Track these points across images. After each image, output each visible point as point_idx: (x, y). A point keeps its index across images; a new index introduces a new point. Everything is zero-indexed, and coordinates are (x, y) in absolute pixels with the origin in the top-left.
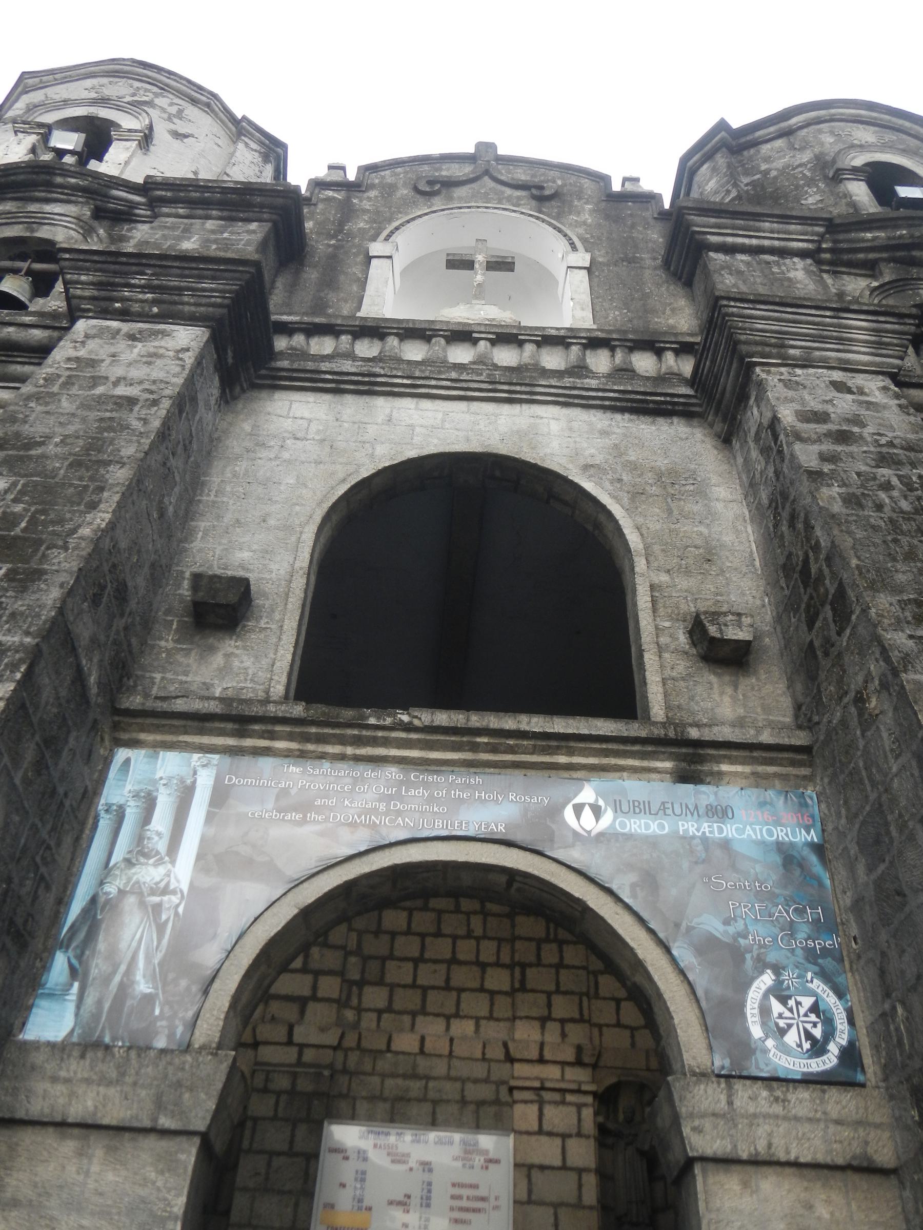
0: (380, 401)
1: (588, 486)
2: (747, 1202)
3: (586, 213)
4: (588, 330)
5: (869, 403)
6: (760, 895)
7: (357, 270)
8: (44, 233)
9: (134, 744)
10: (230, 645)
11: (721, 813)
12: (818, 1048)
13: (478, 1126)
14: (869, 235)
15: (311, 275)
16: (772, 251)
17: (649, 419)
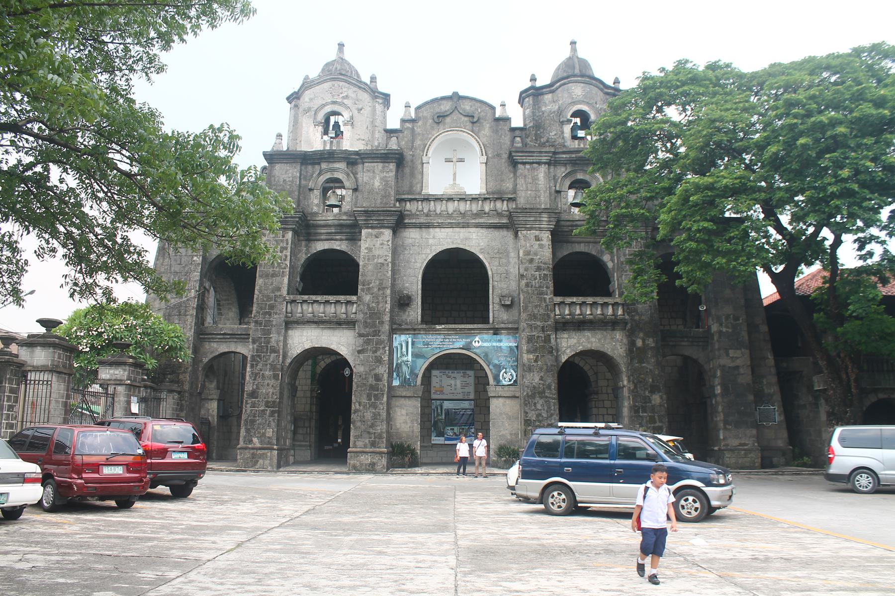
0: (431, 230)
1: (481, 256)
2: (497, 402)
3: (486, 130)
4: (484, 194)
5: (542, 244)
6: (505, 356)
7: (420, 167)
8: (337, 175)
9: (396, 334)
10: (409, 309)
11: (500, 341)
12: (510, 380)
13: (466, 369)
14: (564, 156)
15: (407, 170)
16: (536, 163)
17: (497, 230)
